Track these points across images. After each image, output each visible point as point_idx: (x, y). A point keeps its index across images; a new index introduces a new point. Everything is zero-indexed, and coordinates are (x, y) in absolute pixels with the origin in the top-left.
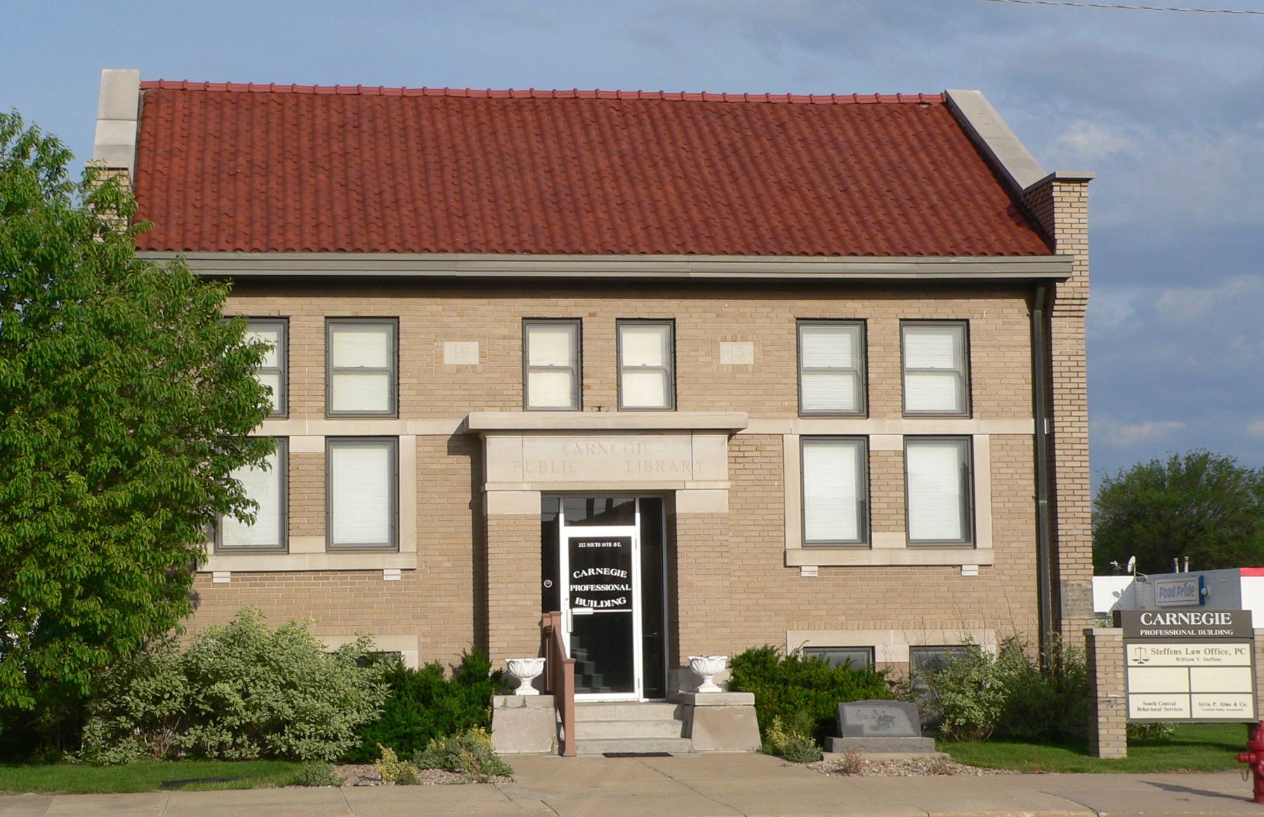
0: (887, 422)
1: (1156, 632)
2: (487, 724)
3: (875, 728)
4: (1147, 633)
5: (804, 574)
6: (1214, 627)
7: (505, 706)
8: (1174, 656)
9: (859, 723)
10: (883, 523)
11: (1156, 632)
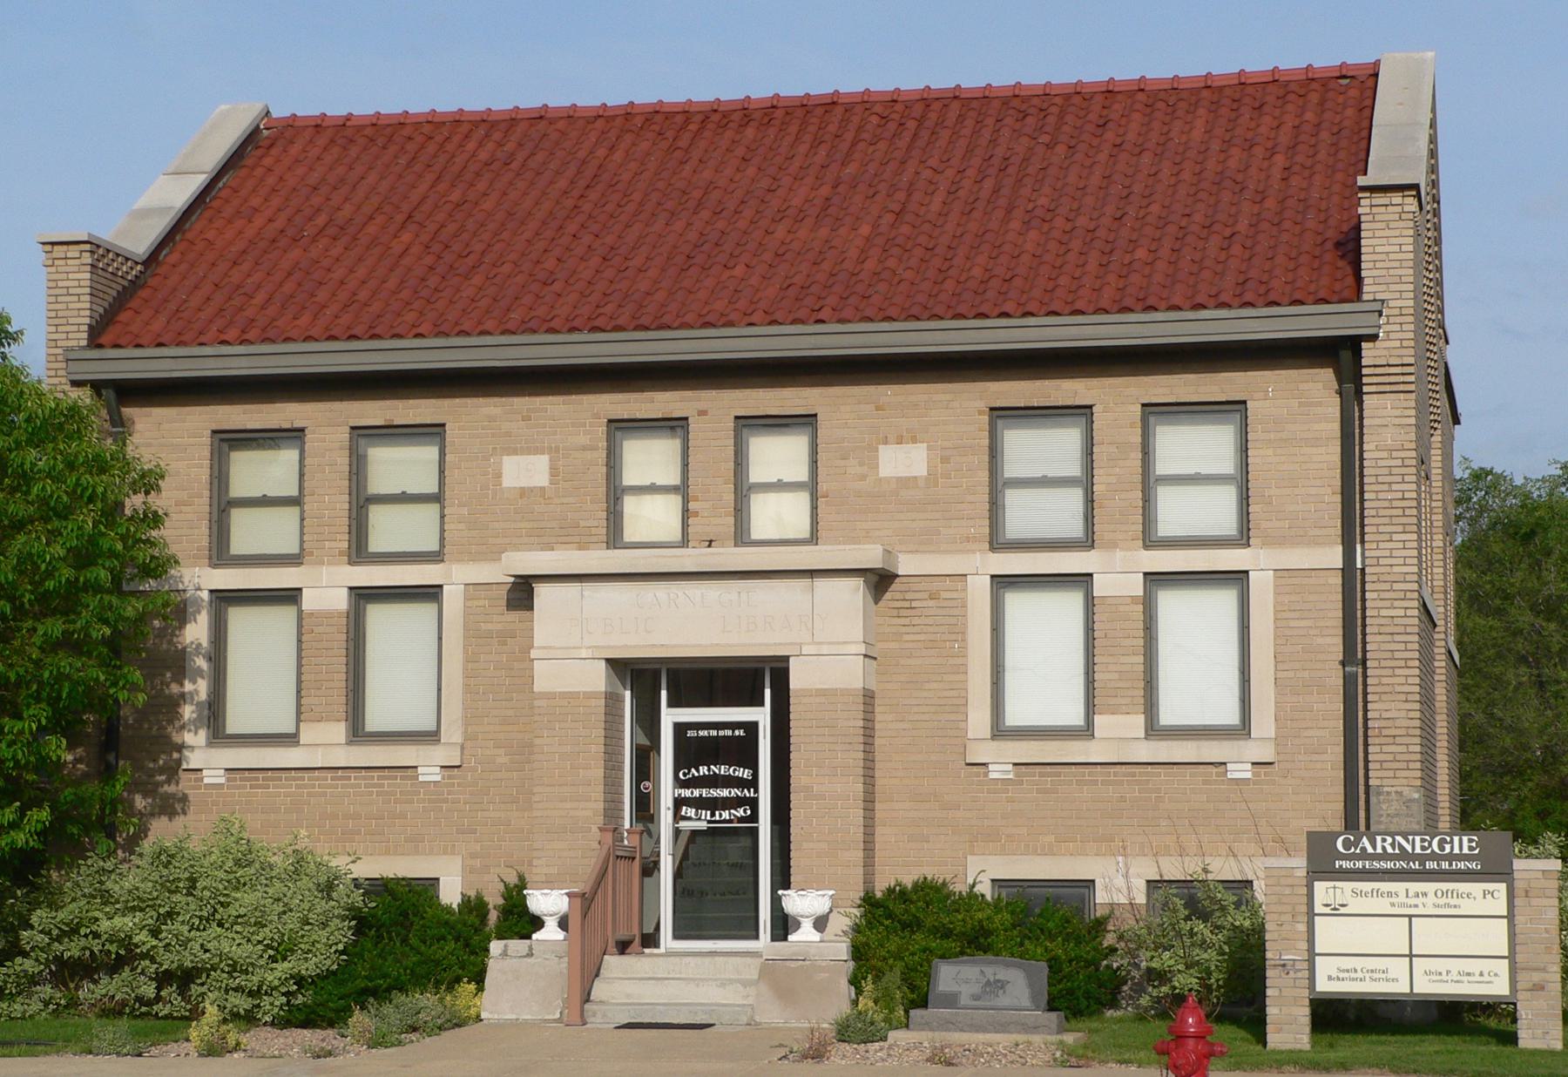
0: (1119, 554)
1: (1359, 864)
2: (479, 979)
3: (976, 997)
4: (1346, 864)
5: (992, 776)
6: (1451, 857)
7: (505, 954)
8: (1387, 900)
9: (955, 988)
10: (1112, 701)
11: (1359, 864)
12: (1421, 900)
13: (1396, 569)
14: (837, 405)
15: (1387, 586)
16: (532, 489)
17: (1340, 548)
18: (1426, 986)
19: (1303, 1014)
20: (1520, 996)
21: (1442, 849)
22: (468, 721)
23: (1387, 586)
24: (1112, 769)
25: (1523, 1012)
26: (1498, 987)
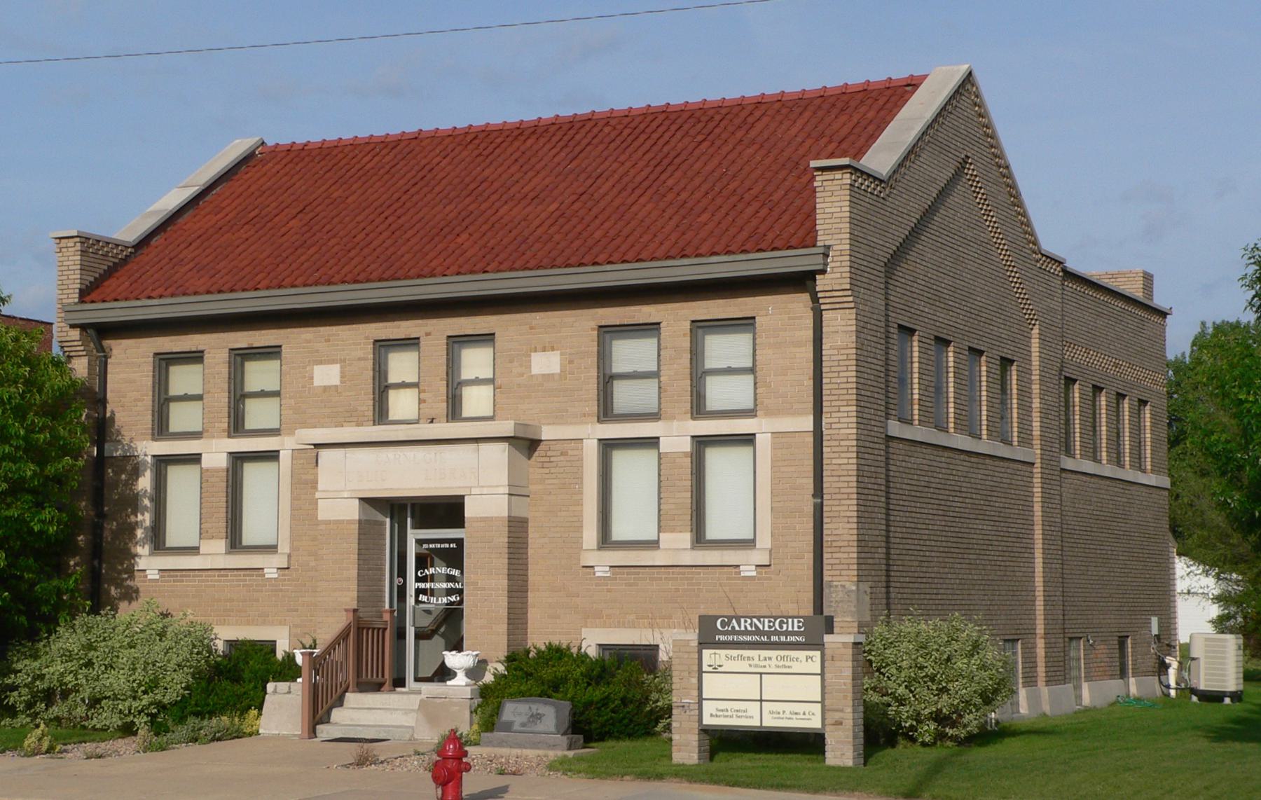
0: (675, 423)
1: (730, 638)
2: (260, 708)
3: (523, 725)
4: (722, 638)
5: (598, 574)
6: (787, 633)
7: (275, 692)
8: (747, 663)
9: (512, 718)
10: (672, 523)
11: (730, 638)
12: (768, 662)
13: (842, 431)
14: (292, 339)
15: (836, 443)
16: (330, 387)
17: (811, 417)
18: (770, 722)
19: (694, 738)
20: (828, 729)
21: (781, 627)
22: (293, 540)
23: (836, 443)
24: (671, 570)
25: (830, 741)
26: (814, 723)
